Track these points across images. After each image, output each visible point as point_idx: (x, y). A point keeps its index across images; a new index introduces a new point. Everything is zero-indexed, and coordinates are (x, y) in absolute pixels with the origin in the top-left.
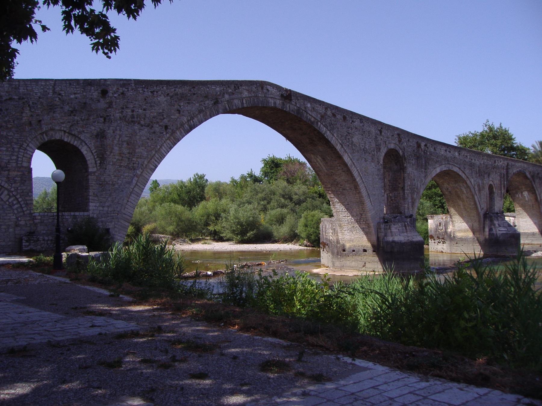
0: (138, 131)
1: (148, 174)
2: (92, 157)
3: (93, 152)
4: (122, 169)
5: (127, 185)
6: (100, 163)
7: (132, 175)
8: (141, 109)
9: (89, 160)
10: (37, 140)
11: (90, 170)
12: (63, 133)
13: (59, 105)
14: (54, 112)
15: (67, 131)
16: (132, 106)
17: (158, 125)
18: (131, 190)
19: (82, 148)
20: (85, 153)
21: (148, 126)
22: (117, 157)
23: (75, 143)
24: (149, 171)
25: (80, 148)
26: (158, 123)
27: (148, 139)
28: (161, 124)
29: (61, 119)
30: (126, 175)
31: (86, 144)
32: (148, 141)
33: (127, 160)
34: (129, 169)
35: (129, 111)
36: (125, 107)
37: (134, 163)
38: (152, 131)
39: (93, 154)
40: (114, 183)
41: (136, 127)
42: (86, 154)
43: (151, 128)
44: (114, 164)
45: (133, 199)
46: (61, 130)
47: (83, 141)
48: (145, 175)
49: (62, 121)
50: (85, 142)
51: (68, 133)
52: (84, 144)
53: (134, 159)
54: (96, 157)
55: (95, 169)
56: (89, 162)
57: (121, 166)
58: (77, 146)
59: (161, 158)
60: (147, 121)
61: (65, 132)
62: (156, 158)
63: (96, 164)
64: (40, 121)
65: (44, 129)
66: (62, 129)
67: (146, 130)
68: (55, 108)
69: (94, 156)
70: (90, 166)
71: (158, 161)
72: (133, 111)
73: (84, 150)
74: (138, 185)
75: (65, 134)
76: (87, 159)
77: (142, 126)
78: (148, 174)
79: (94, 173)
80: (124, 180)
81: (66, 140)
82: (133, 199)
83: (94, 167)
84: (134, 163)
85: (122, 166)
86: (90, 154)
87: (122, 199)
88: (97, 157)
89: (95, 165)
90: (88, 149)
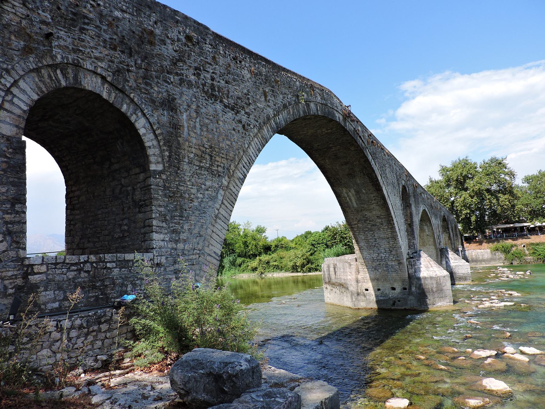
0: (220, 115)
1: (236, 187)
2: (155, 143)
3: (157, 132)
4: (202, 172)
5: (210, 203)
6: (170, 157)
7: (217, 186)
8: (223, 80)
9: (150, 147)
10: (41, 77)
11: (153, 167)
12: (99, 80)
13: (91, 20)
14: (82, 30)
15: (109, 79)
16: (212, 71)
17: (243, 112)
18: (217, 212)
19: (136, 121)
20: (142, 131)
21: (233, 109)
22: (194, 150)
23: (124, 108)
24: (237, 181)
25: (133, 119)
26: (243, 108)
27: (234, 130)
28: (247, 111)
29: (96, 49)
30: (208, 183)
31: (144, 115)
32: (233, 132)
33: (208, 157)
34: (212, 173)
35: (208, 76)
36: (202, 68)
37: (218, 166)
38: (237, 118)
39: (156, 136)
40: (192, 196)
41: (219, 107)
42: (144, 135)
43: (236, 114)
44: (190, 163)
45: (220, 227)
46: (95, 73)
47: (137, 107)
48: (232, 188)
49: (97, 55)
50: (142, 111)
51: (111, 84)
52: (140, 114)
53: (218, 159)
54: (161, 144)
55: (160, 167)
56: (150, 152)
57: (201, 167)
58: (129, 114)
59: (249, 163)
60: (232, 101)
61: (104, 78)
62: (243, 162)
63: (163, 157)
64: (49, 36)
65: (59, 57)
66: (99, 70)
67: (230, 114)
68: (88, 24)
69: (159, 142)
70: (152, 159)
71: (247, 167)
72: (213, 79)
73: (141, 125)
74: (224, 204)
75: (103, 84)
76: (147, 144)
77: (226, 106)
78: (236, 187)
79: (161, 173)
80: (207, 192)
81: (105, 95)
82: (220, 227)
83: (158, 163)
84: (218, 166)
85: (202, 167)
86: (152, 136)
87: (205, 227)
88: (164, 144)
89: (160, 160)
90: (147, 125)
